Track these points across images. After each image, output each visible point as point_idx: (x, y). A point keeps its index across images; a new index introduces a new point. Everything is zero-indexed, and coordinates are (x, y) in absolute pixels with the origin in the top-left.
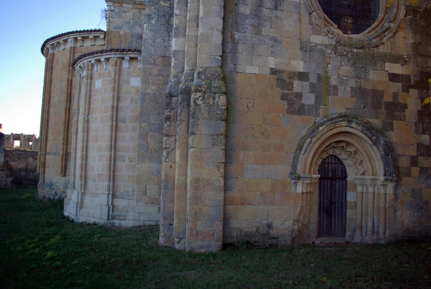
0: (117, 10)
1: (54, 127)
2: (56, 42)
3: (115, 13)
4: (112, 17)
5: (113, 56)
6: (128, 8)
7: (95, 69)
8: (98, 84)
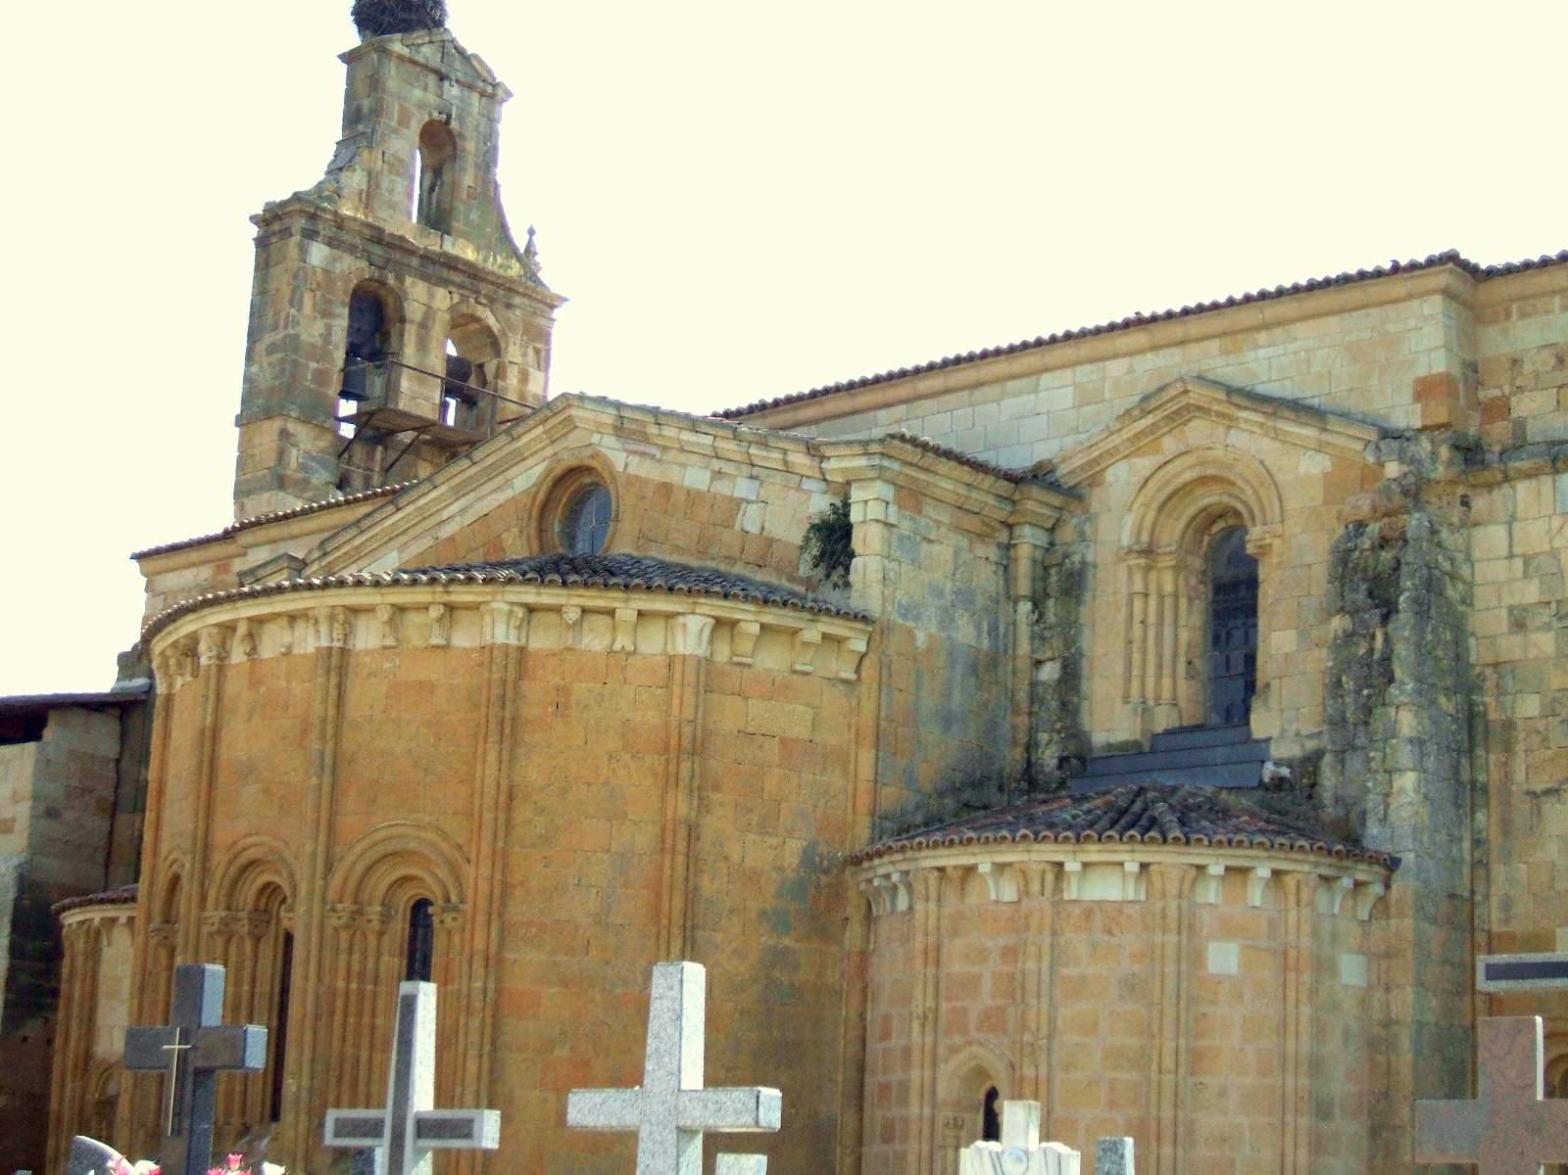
0: (905, 527)
1: (562, 1052)
2: (575, 601)
3: (901, 538)
4: (888, 557)
5: (1306, 868)
6: (939, 524)
7: (1210, 893)
8: (1223, 958)
